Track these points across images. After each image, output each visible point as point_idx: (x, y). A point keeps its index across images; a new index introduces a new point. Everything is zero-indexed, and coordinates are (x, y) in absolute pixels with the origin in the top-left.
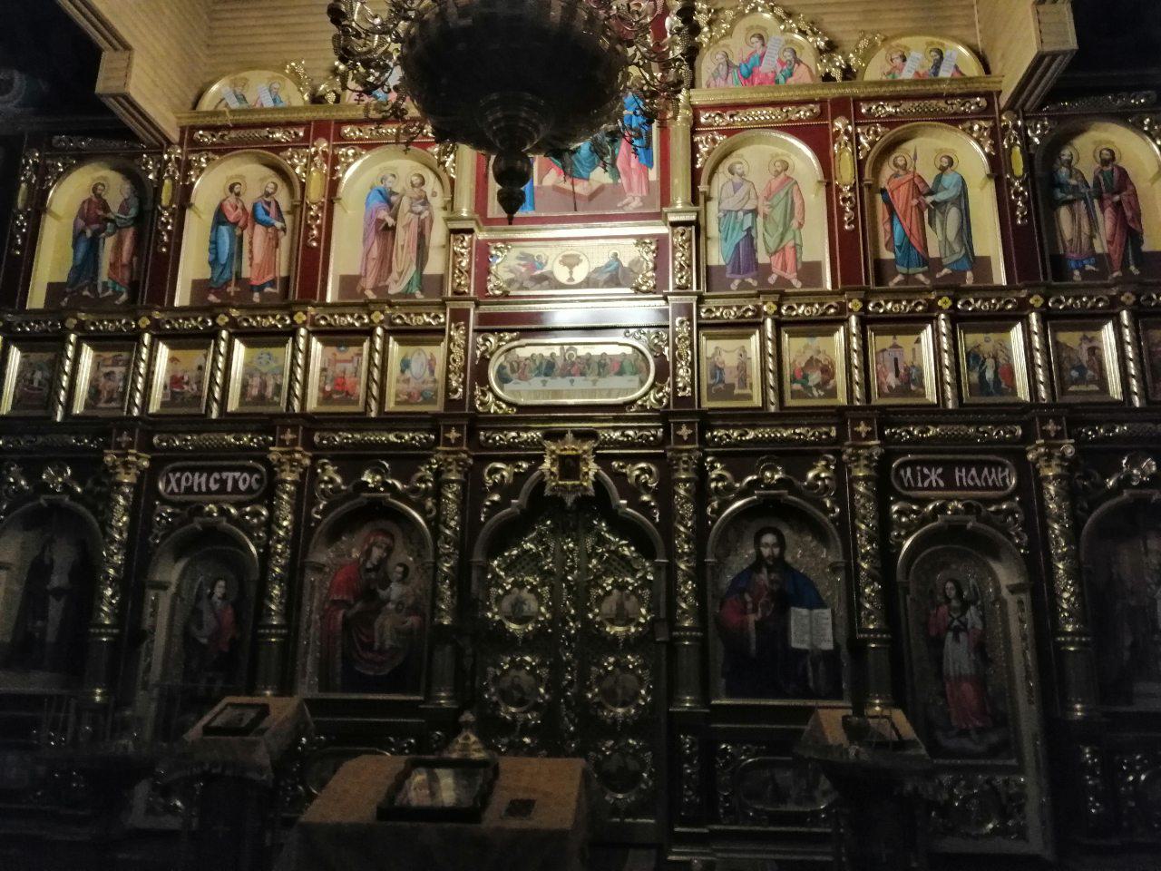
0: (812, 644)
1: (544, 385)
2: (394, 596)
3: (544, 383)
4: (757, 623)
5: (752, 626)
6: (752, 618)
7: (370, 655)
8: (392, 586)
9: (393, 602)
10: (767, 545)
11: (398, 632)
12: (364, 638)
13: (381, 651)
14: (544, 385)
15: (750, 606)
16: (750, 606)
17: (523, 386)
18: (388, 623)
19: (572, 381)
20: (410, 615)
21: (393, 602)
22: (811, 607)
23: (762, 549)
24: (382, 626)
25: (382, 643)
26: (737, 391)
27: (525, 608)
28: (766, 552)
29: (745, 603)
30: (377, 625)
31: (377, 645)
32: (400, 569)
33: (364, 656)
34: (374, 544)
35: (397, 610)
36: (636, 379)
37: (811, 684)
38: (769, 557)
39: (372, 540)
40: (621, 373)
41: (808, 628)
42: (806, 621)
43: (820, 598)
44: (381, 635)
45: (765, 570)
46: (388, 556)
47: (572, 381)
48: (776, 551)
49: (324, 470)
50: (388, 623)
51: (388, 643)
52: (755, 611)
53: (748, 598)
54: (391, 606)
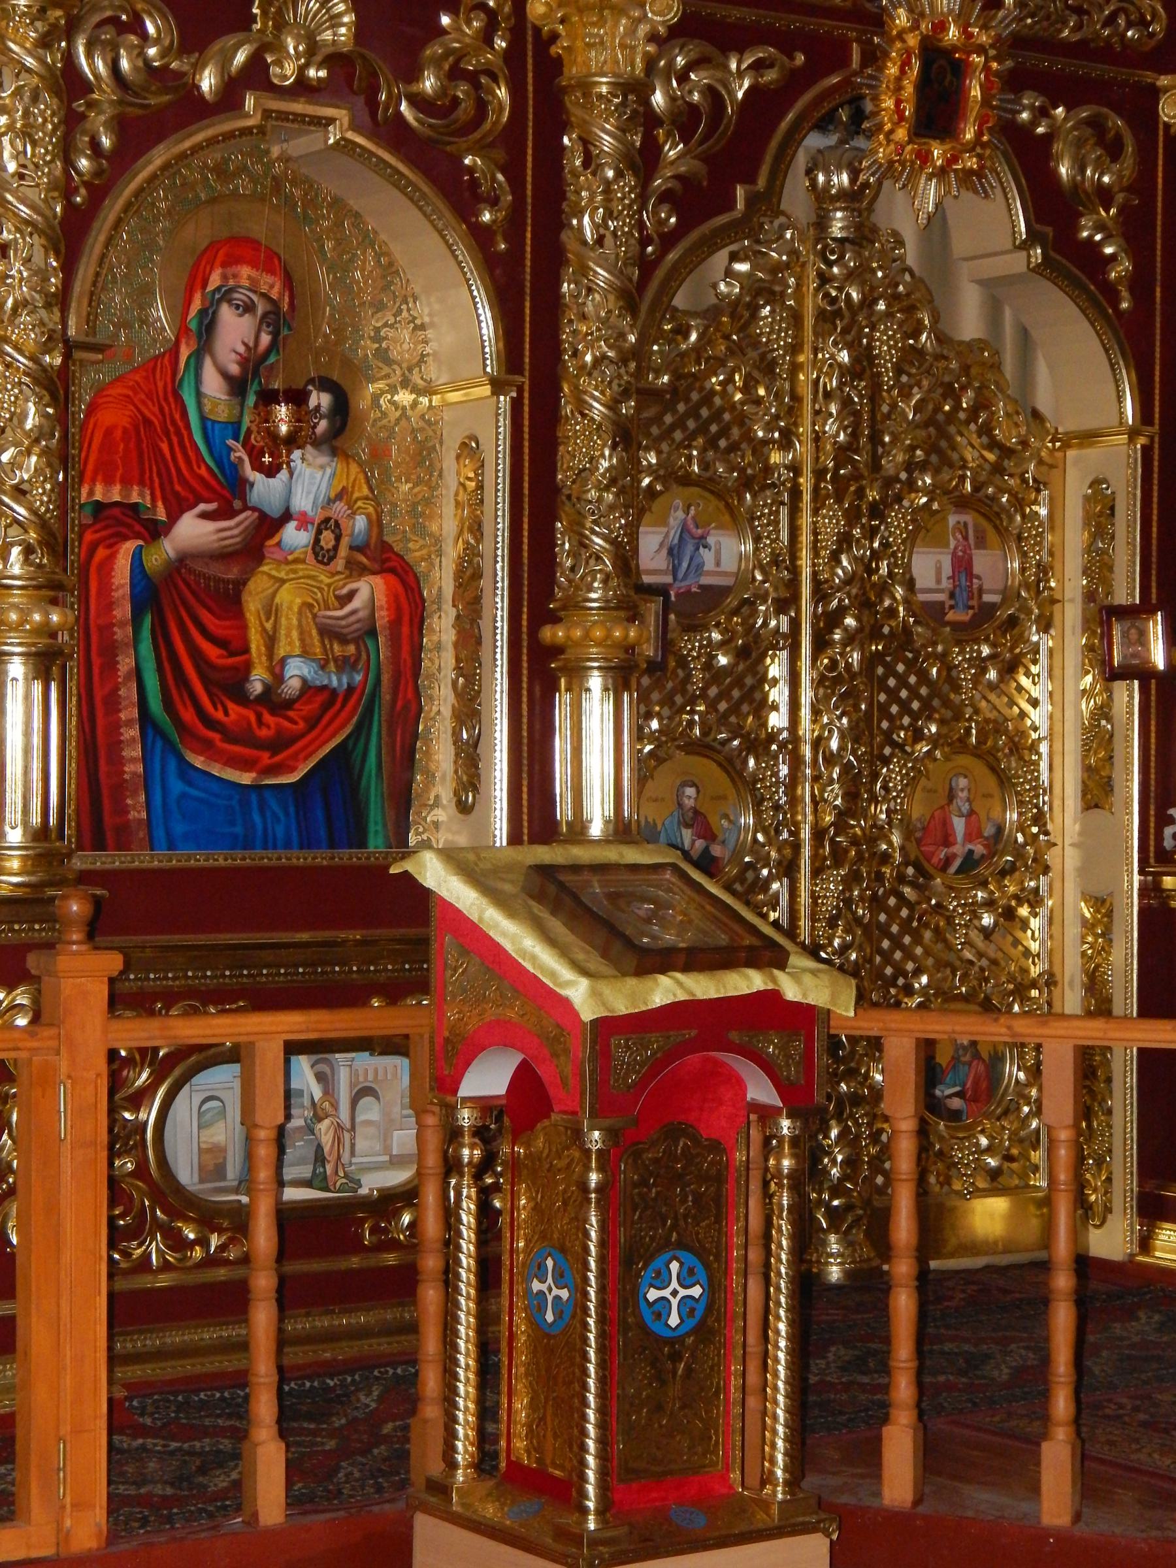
2: (302, 502)
9: (304, 521)
11: (328, 632)
12: (212, 651)
13: (271, 700)
18: (289, 598)
20: (363, 571)
21: (304, 521)
24: (271, 610)
30: (252, 605)
31: (256, 688)
33: (220, 715)
34: (226, 295)
35: (322, 555)
39: (215, 280)
44: (271, 641)
50: (289, 598)
51: (297, 671)
54: (294, 536)
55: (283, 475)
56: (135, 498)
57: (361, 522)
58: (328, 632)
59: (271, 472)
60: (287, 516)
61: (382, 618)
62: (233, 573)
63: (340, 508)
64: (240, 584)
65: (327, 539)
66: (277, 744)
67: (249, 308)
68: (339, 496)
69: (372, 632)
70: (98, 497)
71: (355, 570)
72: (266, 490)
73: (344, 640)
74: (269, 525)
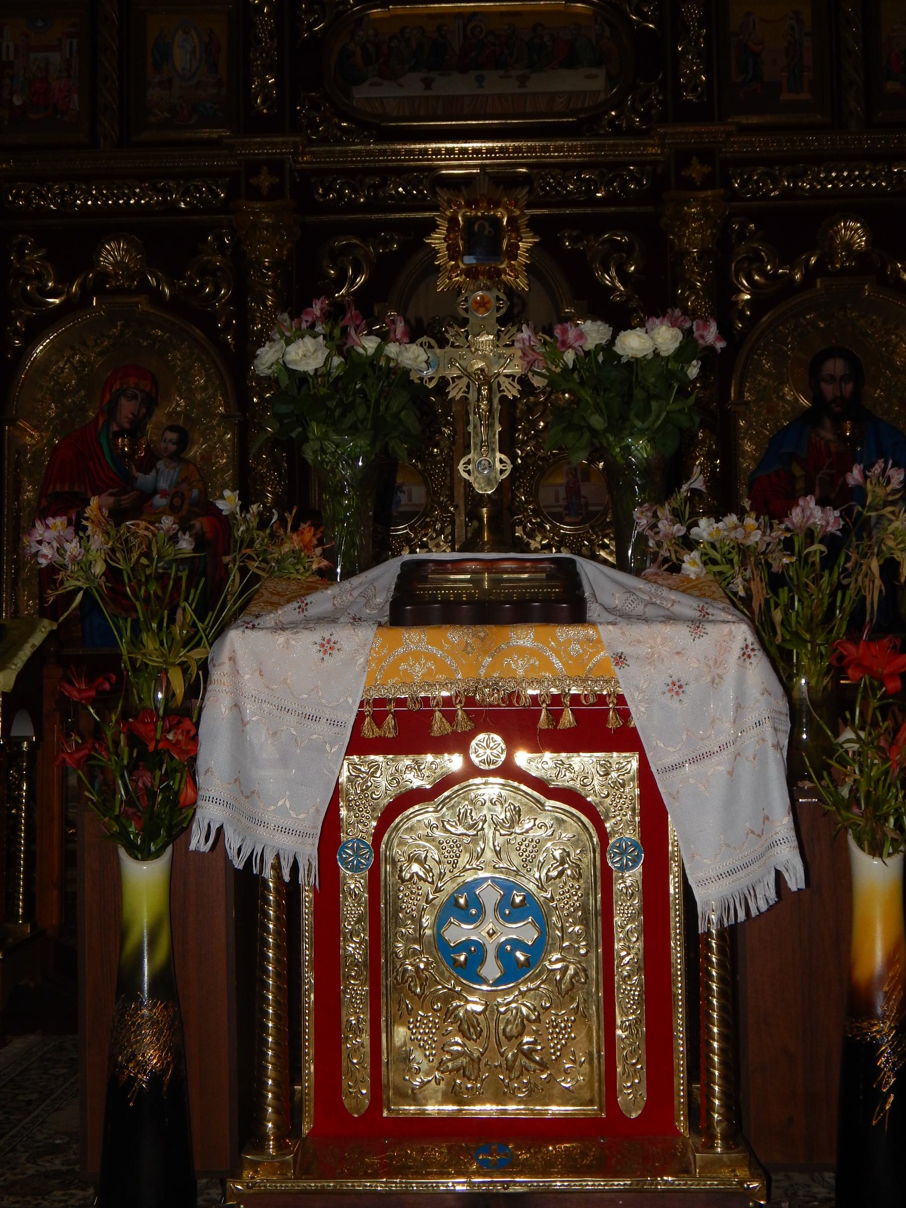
1: (428, 87)
2: (163, 484)
3: (428, 83)
8: (160, 464)
10: (832, 379)
14: (428, 87)
17: (388, 91)
19: (480, 80)
21: (164, 494)
23: (824, 386)
26: (785, 97)
27: (403, 498)
28: (828, 390)
32: (171, 436)
36: (601, 73)
39: (117, 386)
40: (571, 62)
45: (828, 423)
46: (149, 414)
47: (480, 80)
48: (849, 388)
49: (21, 256)
53: (798, 471)
55: (153, 473)
56: (76, 489)
57: (195, 492)
59: (147, 472)
60: (155, 491)
63: (184, 486)
65: (177, 501)
67: (135, 397)
68: (183, 481)
70: (58, 490)
72: (144, 480)
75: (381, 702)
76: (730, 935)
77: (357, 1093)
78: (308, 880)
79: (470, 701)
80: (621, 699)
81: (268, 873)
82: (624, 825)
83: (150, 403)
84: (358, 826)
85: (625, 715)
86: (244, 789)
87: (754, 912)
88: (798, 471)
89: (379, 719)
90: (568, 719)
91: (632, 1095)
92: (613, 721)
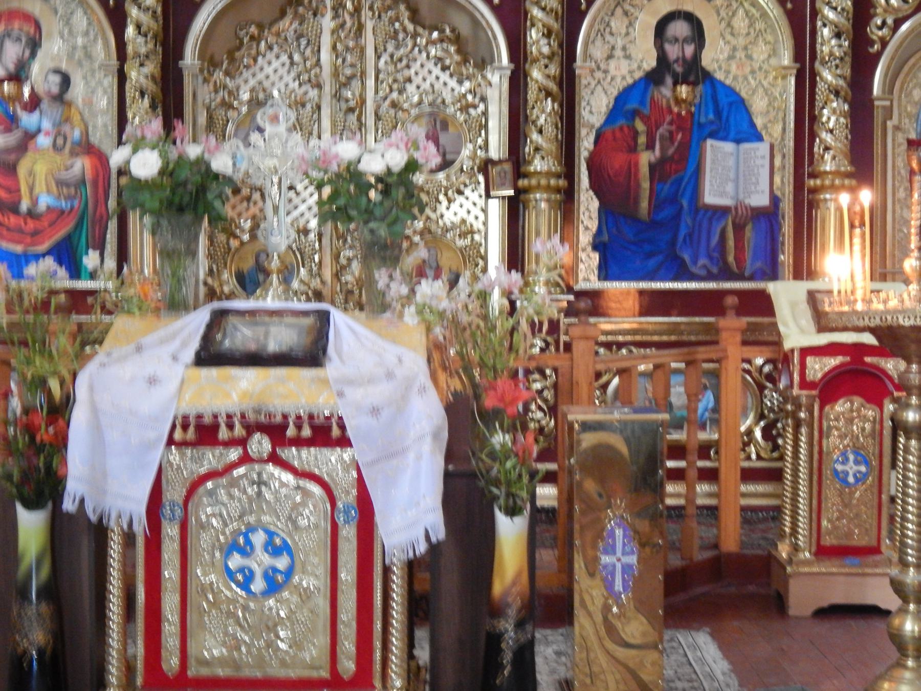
0: (736, 197)
4: (652, 167)
5: (644, 170)
6: (645, 158)
7: (13, 220)
11: (60, 183)
15: (642, 140)
16: (642, 140)
18: (41, 169)
22: (738, 141)
23: (667, 47)
24: (31, 173)
25: (35, 202)
28: (673, 52)
29: (636, 134)
30: (22, 171)
31: (24, 206)
37: (731, 259)
38: (677, 61)
41: (732, 175)
42: (731, 162)
43: (753, 125)
44: (31, 189)
45: (669, 80)
46: (33, 55)
48: (689, 50)
50: (41, 169)
51: (45, 201)
52: (650, 146)
53: (640, 126)
58: (60, 183)
61: (89, 176)
62: (12, 157)
64: (17, 161)
65: (60, 141)
66: (35, 233)
67: (19, 39)
69: (83, 182)
71: (73, 154)
73: (68, 185)
74: (30, 136)
75: (185, 418)
76: (412, 566)
77: (171, 662)
78: (140, 527)
79: (243, 416)
80: (341, 418)
81: (113, 524)
82: (347, 498)
83: (34, 45)
84: (173, 494)
85: (342, 427)
86: (99, 476)
87: (417, 553)
88: (640, 126)
89: (185, 427)
90: (307, 432)
91: (348, 666)
92: (336, 432)
